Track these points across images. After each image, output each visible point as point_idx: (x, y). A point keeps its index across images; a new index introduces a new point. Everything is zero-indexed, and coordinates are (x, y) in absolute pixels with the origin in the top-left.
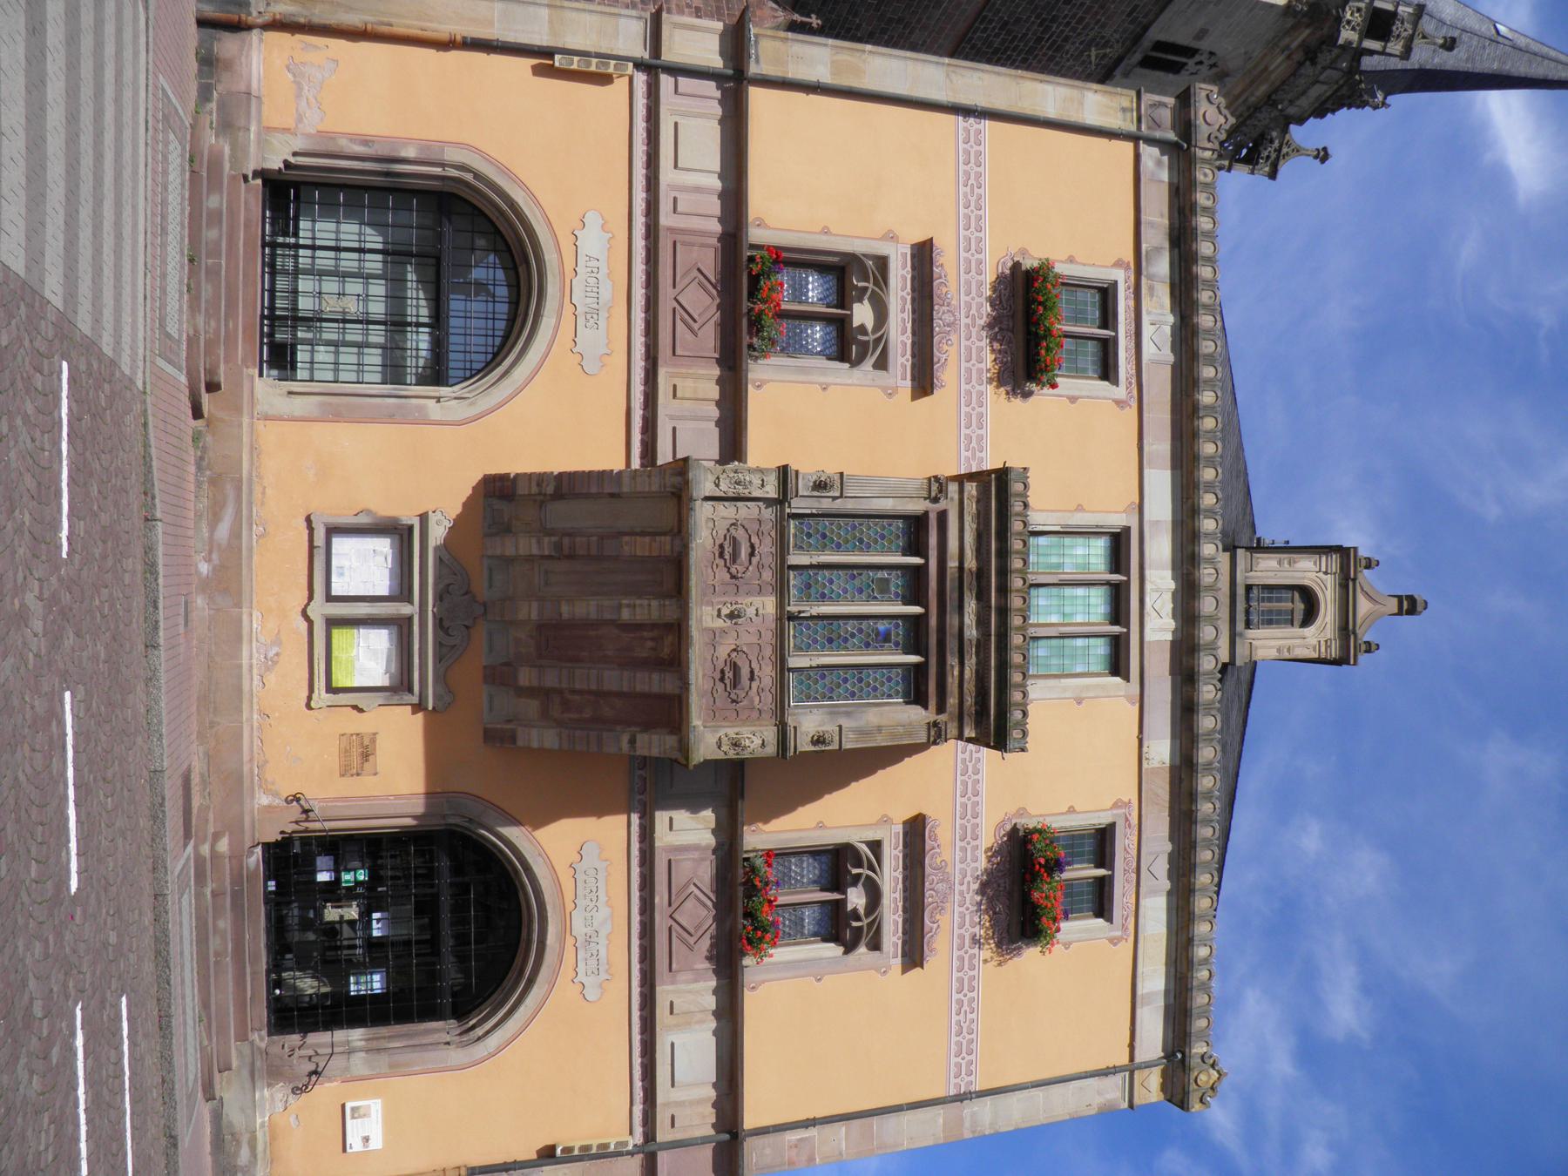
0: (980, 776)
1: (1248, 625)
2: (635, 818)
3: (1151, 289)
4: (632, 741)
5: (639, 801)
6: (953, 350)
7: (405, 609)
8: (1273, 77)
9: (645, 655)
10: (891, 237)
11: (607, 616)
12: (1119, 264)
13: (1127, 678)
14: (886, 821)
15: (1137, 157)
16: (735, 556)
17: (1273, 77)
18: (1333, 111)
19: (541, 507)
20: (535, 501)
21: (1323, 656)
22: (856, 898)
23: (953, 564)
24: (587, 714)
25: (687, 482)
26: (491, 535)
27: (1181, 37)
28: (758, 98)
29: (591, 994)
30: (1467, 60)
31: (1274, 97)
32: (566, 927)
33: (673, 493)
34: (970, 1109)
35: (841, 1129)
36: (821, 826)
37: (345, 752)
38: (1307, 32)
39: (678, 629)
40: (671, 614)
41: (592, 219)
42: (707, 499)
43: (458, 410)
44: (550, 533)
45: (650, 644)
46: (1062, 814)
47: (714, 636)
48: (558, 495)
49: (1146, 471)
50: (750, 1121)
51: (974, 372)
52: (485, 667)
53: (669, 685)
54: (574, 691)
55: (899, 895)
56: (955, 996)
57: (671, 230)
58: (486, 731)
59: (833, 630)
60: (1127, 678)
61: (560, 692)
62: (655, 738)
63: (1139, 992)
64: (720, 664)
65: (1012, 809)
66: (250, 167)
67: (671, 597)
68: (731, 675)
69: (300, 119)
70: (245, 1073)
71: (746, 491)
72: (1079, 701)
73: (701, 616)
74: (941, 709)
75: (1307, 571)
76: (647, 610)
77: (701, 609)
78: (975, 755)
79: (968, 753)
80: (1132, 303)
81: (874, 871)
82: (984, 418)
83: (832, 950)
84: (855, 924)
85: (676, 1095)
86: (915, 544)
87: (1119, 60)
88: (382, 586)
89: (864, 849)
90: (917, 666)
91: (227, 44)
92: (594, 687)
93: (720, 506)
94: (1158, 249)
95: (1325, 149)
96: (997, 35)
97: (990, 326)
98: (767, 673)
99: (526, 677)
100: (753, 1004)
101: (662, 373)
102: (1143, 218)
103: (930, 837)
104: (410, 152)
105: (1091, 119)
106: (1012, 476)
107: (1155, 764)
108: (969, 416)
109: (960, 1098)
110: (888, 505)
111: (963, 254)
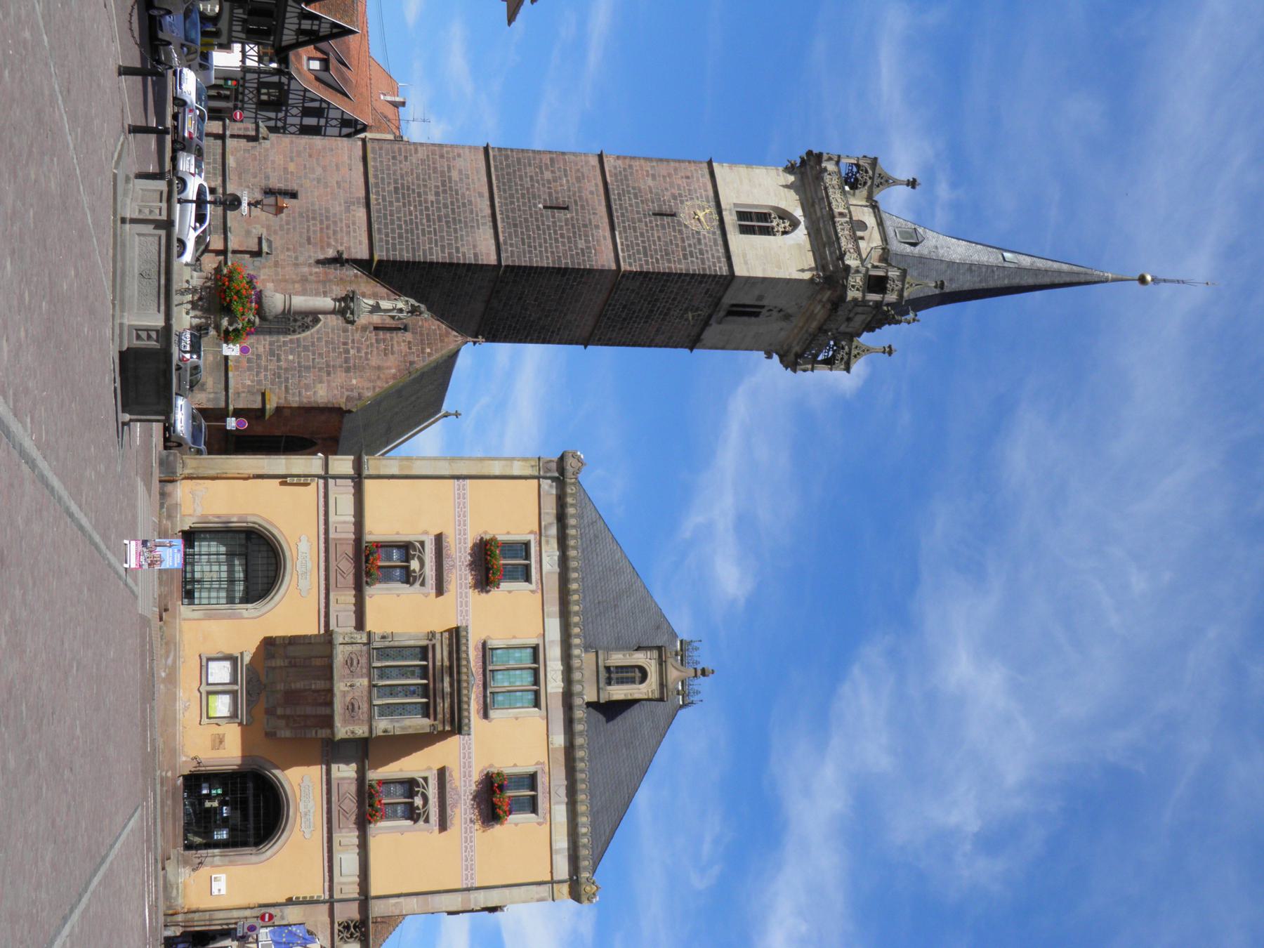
1: (609, 683)
2: (324, 767)
3: (547, 542)
4: (316, 733)
6: (453, 577)
7: (235, 687)
8: (818, 317)
10: (426, 533)
11: (307, 687)
12: (531, 532)
13: (540, 709)
14: (429, 769)
15: (539, 486)
16: (352, 664)
17: (818, 317)
18: (880, 328)
21: (650, 697)
22: (418, 801)
23: (438, 664)
25: (332, 639)
28: (369, 485)
29: (307, 836)
30: (980, 282)
31: (825, 327)
32: (296, 809)
34: (473, 895)
35: (414, 900)
36: (401, 770)
37: (214, 741)
39: (330, 691)
40: (328, 686)
41: (304, 538)
42: (341, 644)
43: (256, 613)
47: (344, 694)
48: (290, 644)
49: (546, 620)
50: (374, 892)
53: (328, 711)
54: (299, 716)
55: (436, 800)
56: (464, 844)
57: (334, 539)
59: (392, 691)
60: (540, 709)
63: (554, 848)
65: (487, 765)
66: (178, 530)
69: (195, 511)
70: (176, 861)
72: (517, 719)
74: (435, 719)
75: (640, 658)
76: (320, 685)
80: (538, 549)
81: (424, 788)
83: (409, 823)
84: (417, 811)
85: (343, 880)
86: (425, 658)
87: (710, 317)
88: (227, 680)
91: (169, 487)
93: (346, 646)
94: (551, 524)
96: (622, 311)
97: (470, 565)
98: (365, 707)
99: (280, 711)
100: (374, 843)
102: (542, 511)
104: (235, 519)
105: (516, 472)
106: (461, 629)
107: (556, 745)
109: (468, 890)
110: (412, 643)
111: (458, 537)
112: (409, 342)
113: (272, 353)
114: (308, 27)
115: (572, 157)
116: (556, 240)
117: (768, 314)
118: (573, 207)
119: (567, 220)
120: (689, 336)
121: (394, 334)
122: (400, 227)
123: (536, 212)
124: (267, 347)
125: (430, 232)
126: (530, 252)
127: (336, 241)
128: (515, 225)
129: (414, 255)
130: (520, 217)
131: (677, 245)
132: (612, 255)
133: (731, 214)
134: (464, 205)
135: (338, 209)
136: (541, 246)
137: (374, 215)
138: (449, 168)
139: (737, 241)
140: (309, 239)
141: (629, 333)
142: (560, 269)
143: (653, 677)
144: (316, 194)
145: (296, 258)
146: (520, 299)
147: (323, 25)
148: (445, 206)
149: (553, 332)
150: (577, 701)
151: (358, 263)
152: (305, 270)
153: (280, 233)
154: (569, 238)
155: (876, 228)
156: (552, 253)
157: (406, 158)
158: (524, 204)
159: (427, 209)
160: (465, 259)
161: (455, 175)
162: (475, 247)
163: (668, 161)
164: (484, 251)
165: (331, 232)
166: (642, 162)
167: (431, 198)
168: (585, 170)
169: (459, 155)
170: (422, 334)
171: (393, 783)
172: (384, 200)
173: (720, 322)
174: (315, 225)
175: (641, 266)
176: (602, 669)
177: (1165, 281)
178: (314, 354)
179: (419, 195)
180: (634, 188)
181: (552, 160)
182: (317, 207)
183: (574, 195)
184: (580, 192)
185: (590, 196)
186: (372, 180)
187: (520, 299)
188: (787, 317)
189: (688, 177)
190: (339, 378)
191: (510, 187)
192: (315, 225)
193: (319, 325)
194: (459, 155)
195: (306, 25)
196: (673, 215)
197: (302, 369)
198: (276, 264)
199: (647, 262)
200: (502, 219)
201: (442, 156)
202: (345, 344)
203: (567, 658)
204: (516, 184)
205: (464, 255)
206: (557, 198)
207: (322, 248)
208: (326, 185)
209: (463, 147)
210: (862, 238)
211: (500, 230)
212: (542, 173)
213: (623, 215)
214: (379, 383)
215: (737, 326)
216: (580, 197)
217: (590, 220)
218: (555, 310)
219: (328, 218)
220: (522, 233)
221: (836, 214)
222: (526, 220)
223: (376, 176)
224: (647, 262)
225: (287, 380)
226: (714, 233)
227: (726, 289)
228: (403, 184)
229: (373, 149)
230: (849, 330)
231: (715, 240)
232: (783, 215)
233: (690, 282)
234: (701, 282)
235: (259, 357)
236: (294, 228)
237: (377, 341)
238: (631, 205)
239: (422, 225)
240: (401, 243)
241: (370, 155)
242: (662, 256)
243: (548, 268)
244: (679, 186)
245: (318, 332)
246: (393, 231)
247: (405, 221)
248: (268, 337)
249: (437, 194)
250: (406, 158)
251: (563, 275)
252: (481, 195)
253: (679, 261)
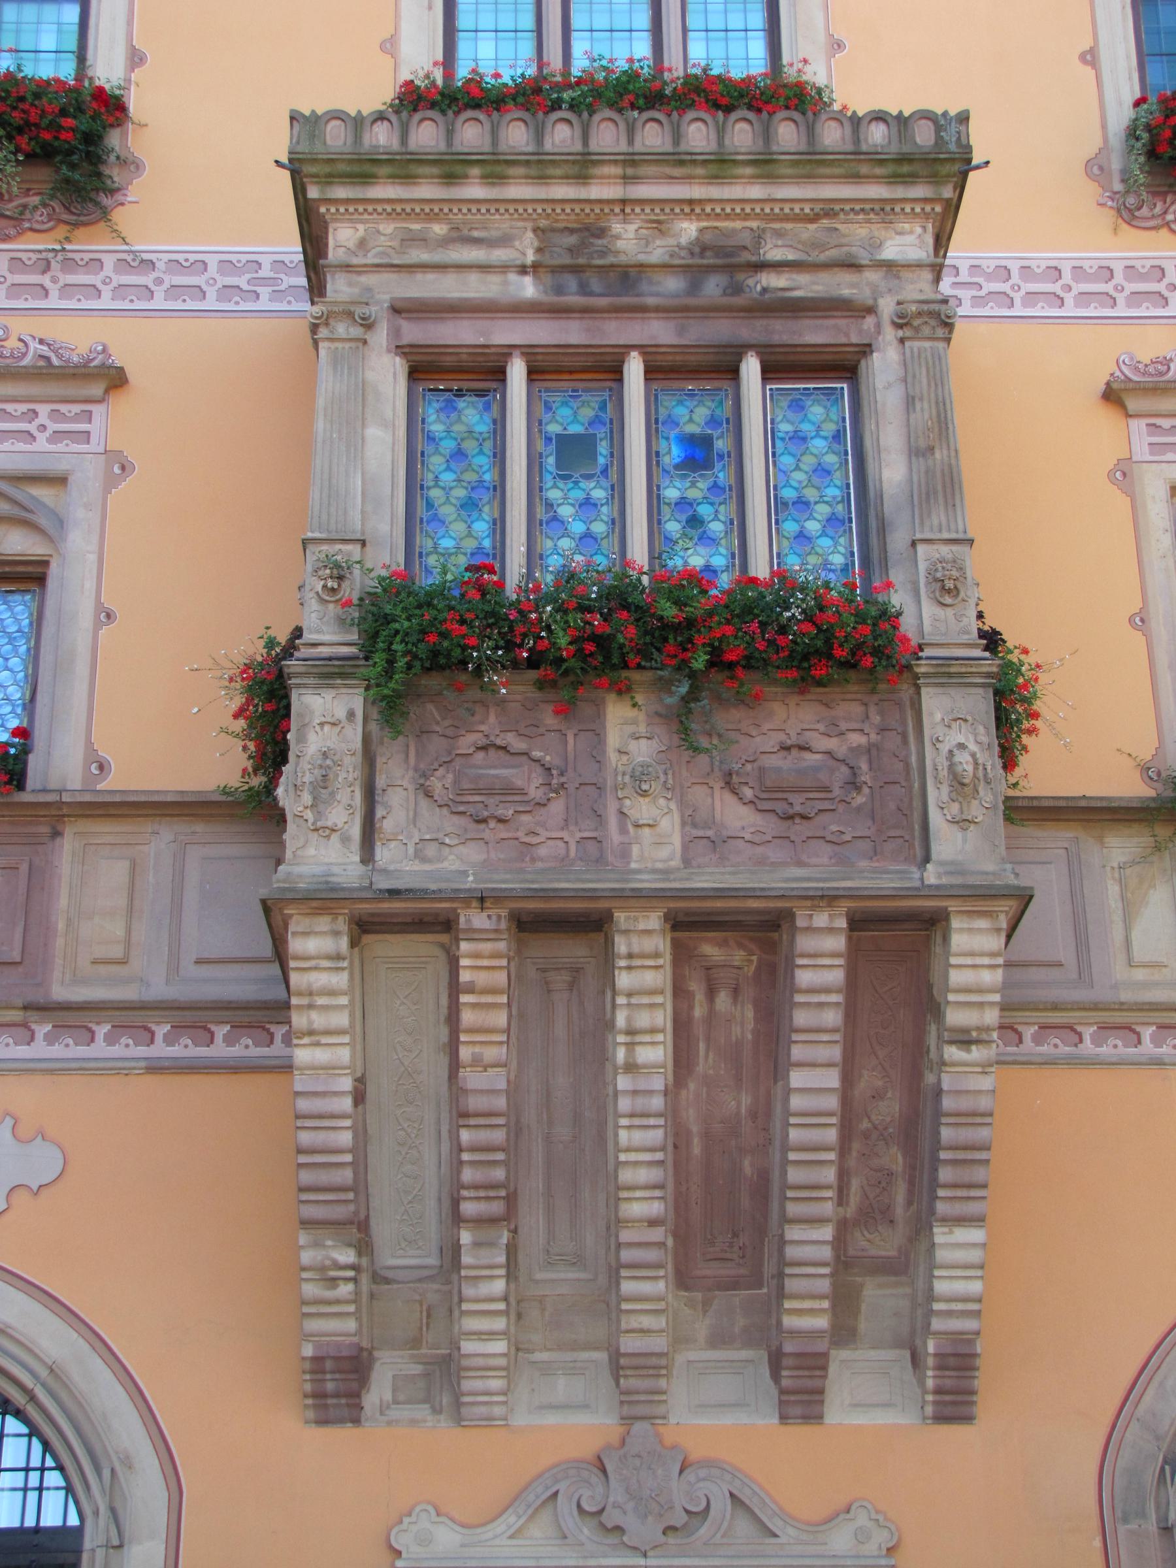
0: (1014, 267)
4: (965, 1039)
5: (1097, 1042)
9: (750, 1014)
16: (509, 791)
19: (387, 1281)
20: (372, 1296)
23: (528, 288)
24: (894, 1159)
26: (458, 1405)
33: (353, 944)
44: (452, 1253)
45: (723, 1000)
46: (1098, 78)
51: (72, 279)
52: (784, 1418)
58: (941, 1418)
61: (843, 1228)
62: (956, 977)
64: (770, 826)
67: (609, 943)
68: (797, 800)
71: (348, 760)
73: (655, 871)
77: (638, 871)
78: (964, 276)
79: (959, 293)
82: (180, 257)
90: (769, 372)
92: (831, 1136)
101: (60, 992)
103: (1161, 374)
108: (175, 291)
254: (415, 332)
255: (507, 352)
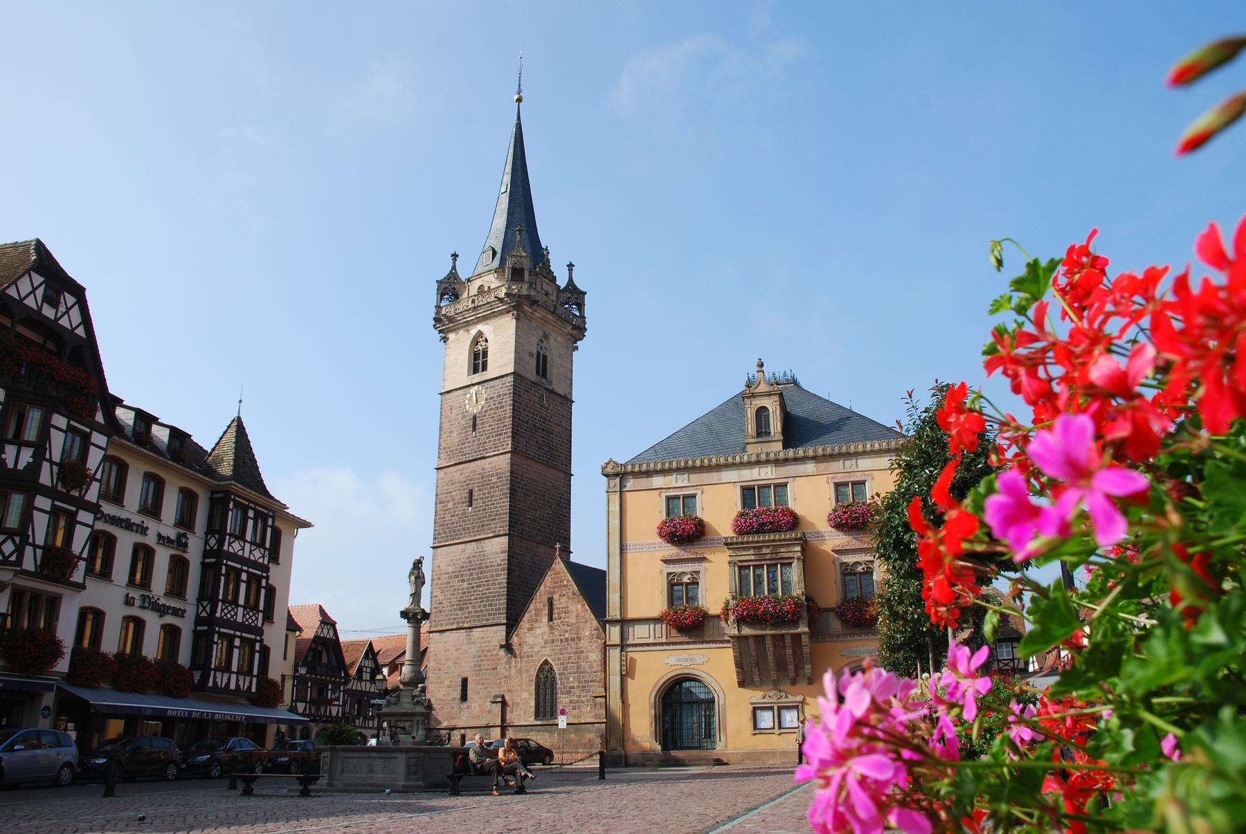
7: (776, 708)
10: (661, 571)
12: (660, 496)
23: (752, 557)
27: (533, 363)
30: (520, 207)
31: (552, 310)
38: (525, 307)
54: (795, 661)
72: (795, 499)
75: (750, 414)
87: (547, 389)
88: (771, 713)
89: (843, 568)
91: (631, 760)
95: (568, 266)
104: (653, 712)
112: (560, 596)
113: (569, 692)
114: (368, 675)
115: (439, 489)
116: (492, 497)
117: (544, 350)
118: (470, 487)
119: (479, 490)
120: (561, 403)
121: (555, 607)
122: (485, 606)
123: (475, 512)
124: (564, 696)
125: (488, 585)
126: (500, 514)
127: (494, 650)
128: (483, 526)
129: (503, 595)
130: (477, 523)
131: (495, 413)
132: (501, 456)
133: (474, 378)
134: (470, 562)
135: (473, 649)
136: (496, 507)
137: (478, 624)
138: (446, 573)
139: (491, 372)
140: (493, 669)
141: (561, 445)
142: (511, 493)
143: (765, 402)
144: (464, 665)
145: (506, 677)
146: (535, 521)
147: (367, 665)
148: (471, 574)
149: (561, 498)
150: (782, 455)
151: (509, 635)
152: (513, 671)
153: (490, 689)
154: (490, 488)
155: (483, 278)
156: (500, 499)
157: (440, 603)
158: (469, 520)
159: (473, 587)
160: (505, 560)
161: (451, 569)
162: (497, 553)
163: (441, 423)
164: (500, 546)
165: (489, 654)
166: (441, 441)
167: (465, 585)
168: (447, 479)
169: (439, 567)
170: (554, 587)
171: (845, 587)
172: (467, 618)
173: (551, 382)
174: (484, 665)
175: (508, 437)
176: (760, 440)
177: (519, 86)
178: (569, 663)
179: (464, 593)
180: (458, 445)
181: (441, 503)
182: (472, 664)
183: (463, 486)
184: (461, 482)
185: (464, 475)
186: (455, 627)
187: (535, 521)
188: (546, 336)
189: (451, 409)
190: (584, 644)
191: (459, 531)
192: (484, 665)
193: (549, 659)
194: (439, 567)
195: (366, 676)
196: (475, 418)
197: (579, 671)
198: (510, 691)
199: (506, 433)
200: (479, 535)
201: (439, 579)
202: (562, 641)
203: (750, 464)
204: (457, 526)
205: (502, 560)
206: (465, 498)
207: (499, 659)
208: (459, 658)
209: (433, 564)
210: (489, 287)
211: (486, 536)
212: (449, 509)
213: (476, 452)
214: (587, 616)
215: (554, 371)
216: (465, 482)
217: (479, 474)
218: (544, 496)
219: (480, 656)
220: (487, 521)
221: (473, 306)
222: (479, 518)
223: (453, 624)
224: (506, 433)
225: (586, 681)
226: (487, 388)
227: (525, 378)
228: (457, 605)
229: (435, 626)
230: (555, 294)
231: (492, 387)
232: (475, 342)
233: (520, 403)
234: (520, 396)
235: (571, 702)
236: (486, 679)
237: (560, 618)
238: (469, 447)
239: (483, 590)
240: (495, 605)
241: (439, 628)
242: (502, 423)
243: (510, 501)
244: (457, 415)
245: (554, 661)
246: (487, 610)
247: (481, 602)
248: (558, 696)
249: (463, 581)
250: (440, 603)
251: (516, 491)
252: (464, 550)
253: (505, 411)
254: (739, 564)
255: (750, 566)
